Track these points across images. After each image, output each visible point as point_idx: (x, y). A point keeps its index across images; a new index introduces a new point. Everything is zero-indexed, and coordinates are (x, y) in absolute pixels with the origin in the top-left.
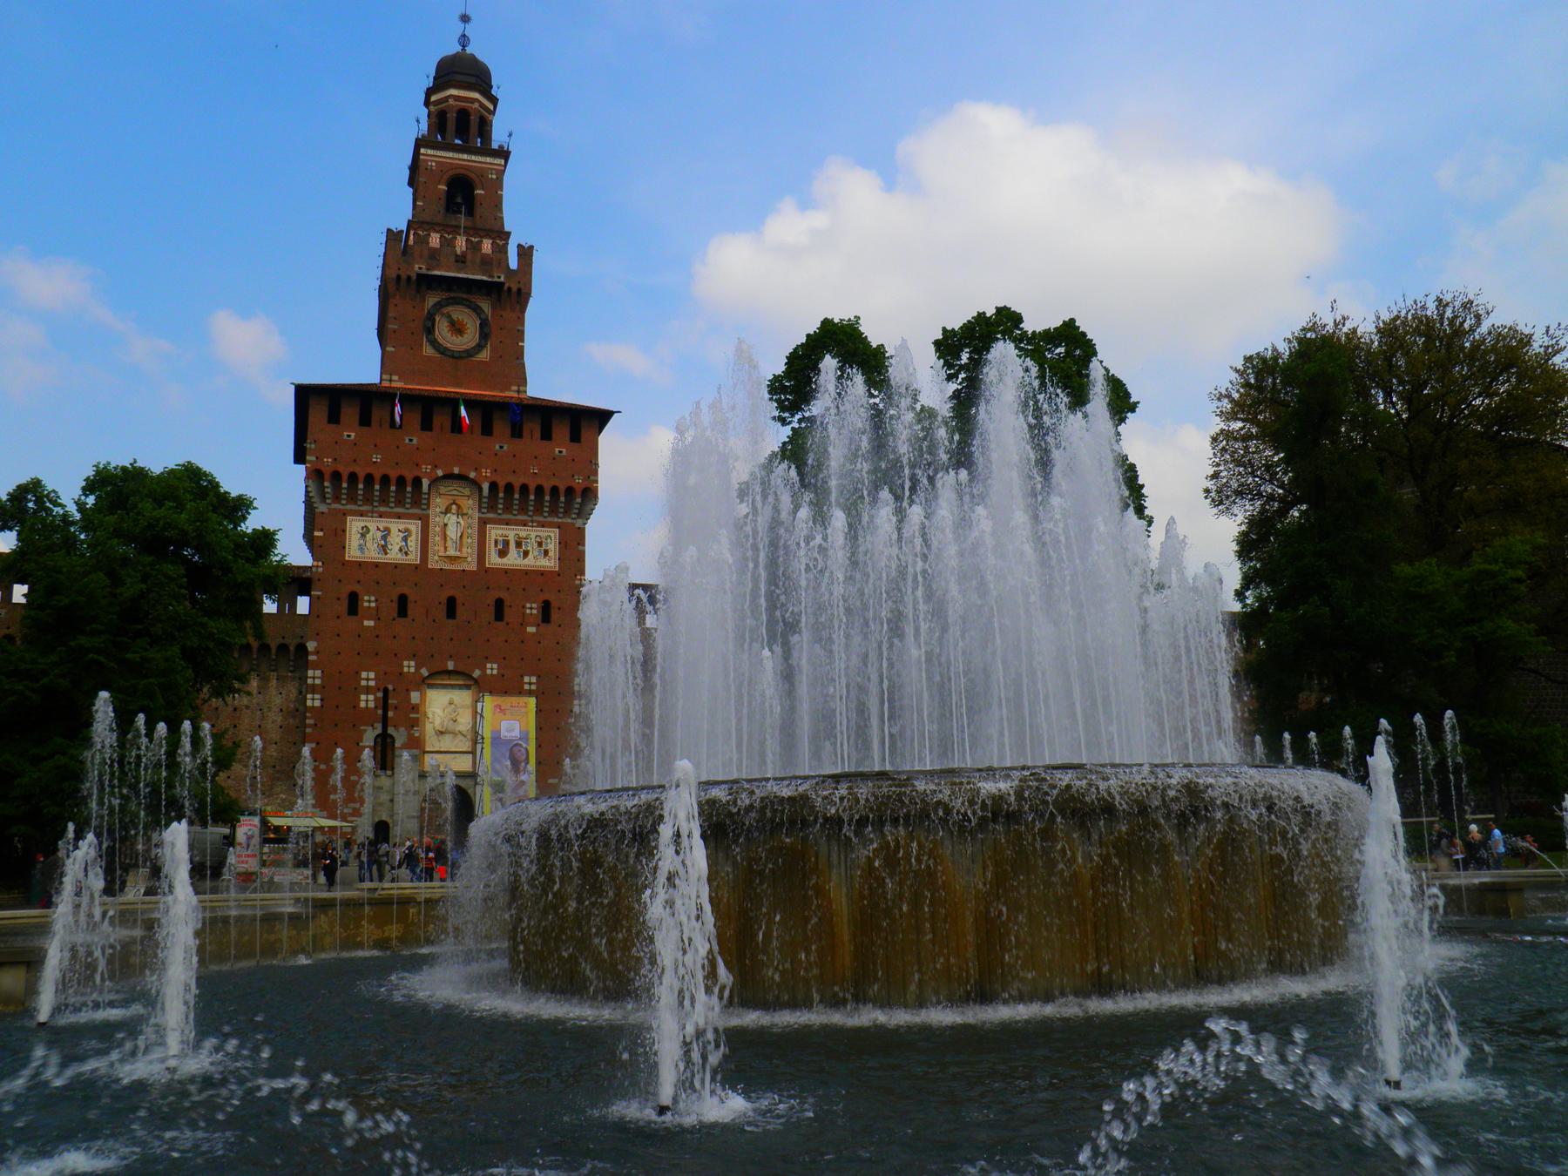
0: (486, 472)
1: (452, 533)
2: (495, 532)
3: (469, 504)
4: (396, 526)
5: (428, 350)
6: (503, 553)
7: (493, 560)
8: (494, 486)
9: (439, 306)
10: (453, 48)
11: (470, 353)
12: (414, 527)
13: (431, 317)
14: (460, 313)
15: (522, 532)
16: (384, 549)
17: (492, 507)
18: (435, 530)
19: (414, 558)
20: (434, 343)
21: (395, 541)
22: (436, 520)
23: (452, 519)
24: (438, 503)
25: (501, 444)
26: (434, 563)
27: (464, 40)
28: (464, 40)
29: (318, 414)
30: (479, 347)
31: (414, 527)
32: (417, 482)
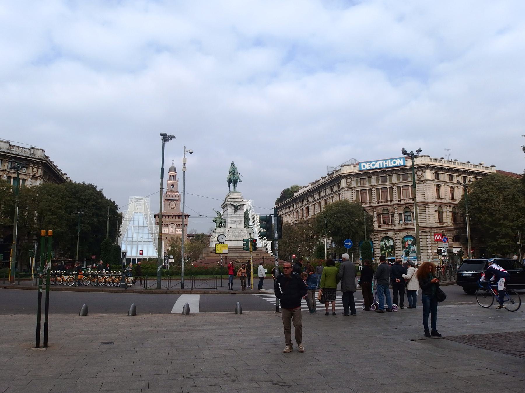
0: (175, 223)
1: (172, 230)
2: (177, 229)
3: (174, 226)
4: (166, 229)
5: (169, 208)
6: (177, 232)
7: (176, 233)
8: (176, 224)
9: (170, 202)
10: (172, 165)
11: (173, 208)
12: (168, 229)
13: (169, 204)
14: (172, 203)
15: (180, 229)
16: (164, 232)
17: (176, 227)
18: (170, 229)
19: (168, 233)
20: (170, 207)
21: (166, 231)
22: (170, 228)
23: (172, 228)
24: (170, 226)
25: (177, 219)
26: (170, 233)
27: (173, 164)
28: (173, 164)
29: (157, 217)
30: (175, 207)
31: (168, 229)
32: (168, 224)
